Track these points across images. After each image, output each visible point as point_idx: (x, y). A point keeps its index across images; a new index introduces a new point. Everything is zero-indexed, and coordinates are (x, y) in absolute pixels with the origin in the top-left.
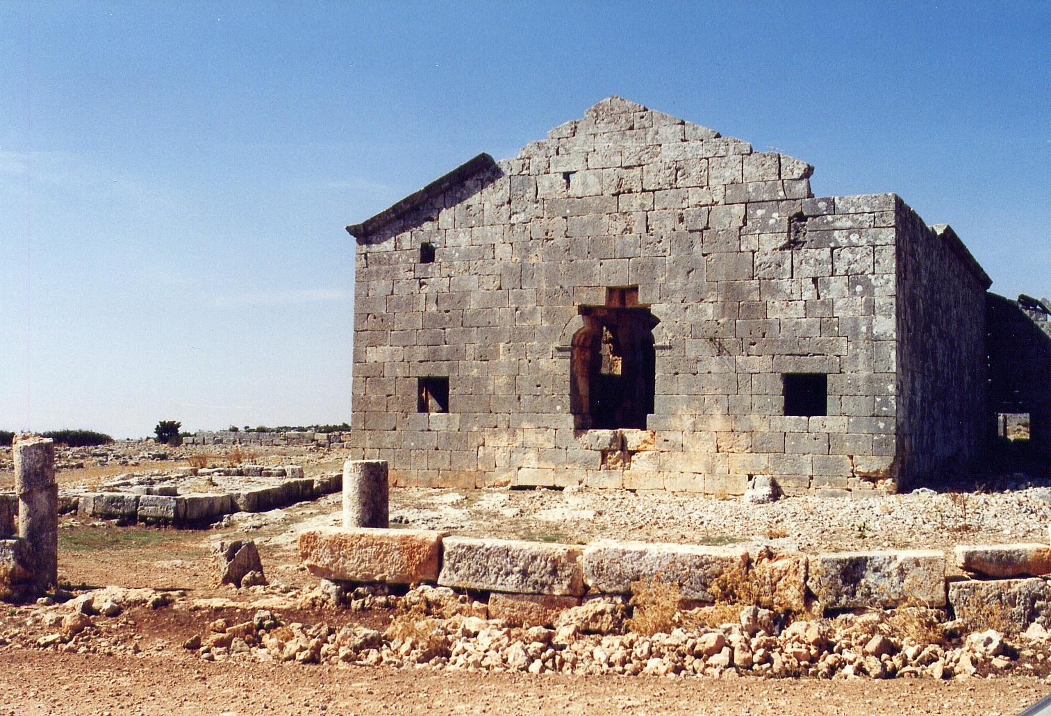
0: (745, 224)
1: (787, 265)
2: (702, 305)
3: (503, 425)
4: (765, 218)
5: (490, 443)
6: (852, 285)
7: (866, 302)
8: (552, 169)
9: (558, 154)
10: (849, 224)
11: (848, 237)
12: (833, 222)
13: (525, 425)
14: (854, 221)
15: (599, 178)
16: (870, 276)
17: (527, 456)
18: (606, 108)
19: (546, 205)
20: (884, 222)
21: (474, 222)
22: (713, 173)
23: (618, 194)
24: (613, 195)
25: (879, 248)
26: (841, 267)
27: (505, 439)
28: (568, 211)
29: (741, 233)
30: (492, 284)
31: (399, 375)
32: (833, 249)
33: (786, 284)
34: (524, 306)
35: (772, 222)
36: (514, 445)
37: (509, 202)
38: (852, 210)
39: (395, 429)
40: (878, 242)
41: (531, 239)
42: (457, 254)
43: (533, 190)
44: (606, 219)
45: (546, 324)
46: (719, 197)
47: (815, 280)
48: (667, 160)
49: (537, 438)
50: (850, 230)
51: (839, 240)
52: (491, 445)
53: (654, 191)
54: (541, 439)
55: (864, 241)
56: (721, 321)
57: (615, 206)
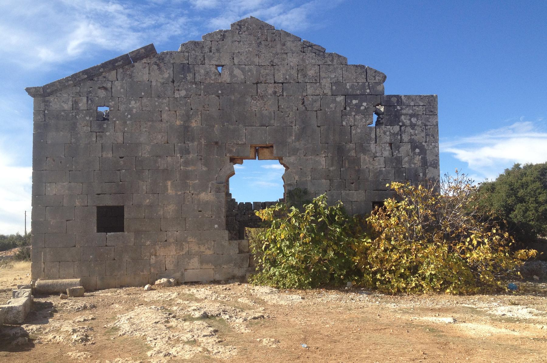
0: (345, 109)
1: (373, 136)
2: (317, 159)
3: (172, 240)
4: (358, 106)
5: (161, 252)
6: (413, 148)
7: (422, 158)
8: (207, 61)
9: (211, 51)
10: (411, 111)
11: (410, 120)
12: (402, 109)
13: (190, 239)
14: (413, 110)
15: (242, 71)
16: (424, 143)
17: (192, 261)
18: (247, 24)
19: (202, 86)
20: (432, 111)
21: (143, 94)
22: (323, 75)
23: (257, 83)
24: (254, 84)
25: (429, 127)
26: (406, 138)
27: (174, 250)
28: (220, 92)
29: (344, 114)
30: (160, 138)
31: (78, 204)
32: (401, 126)
33: (373, 146)
34: (187, 156)
35: (362, 108)
36: (181, 253)
37: (173, 82)
38: (412, 104)
39: (75, 246)
40: (428, 124)
41: (191, 109)
42: (129, 116)
43: (191, 75)
44: (249, 99)
45: (205, 169)
46: (328, 91)
47: (391, 144)
48: (292, 64)
49: (199, 247)
50: (412, 116)
51: (405, 121)
52: (162, 254)
53: (282, 83)
54: (203, 249)
55: (420, 123)
56: (331, 169)
57: (254, 92)
